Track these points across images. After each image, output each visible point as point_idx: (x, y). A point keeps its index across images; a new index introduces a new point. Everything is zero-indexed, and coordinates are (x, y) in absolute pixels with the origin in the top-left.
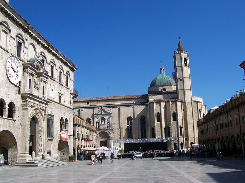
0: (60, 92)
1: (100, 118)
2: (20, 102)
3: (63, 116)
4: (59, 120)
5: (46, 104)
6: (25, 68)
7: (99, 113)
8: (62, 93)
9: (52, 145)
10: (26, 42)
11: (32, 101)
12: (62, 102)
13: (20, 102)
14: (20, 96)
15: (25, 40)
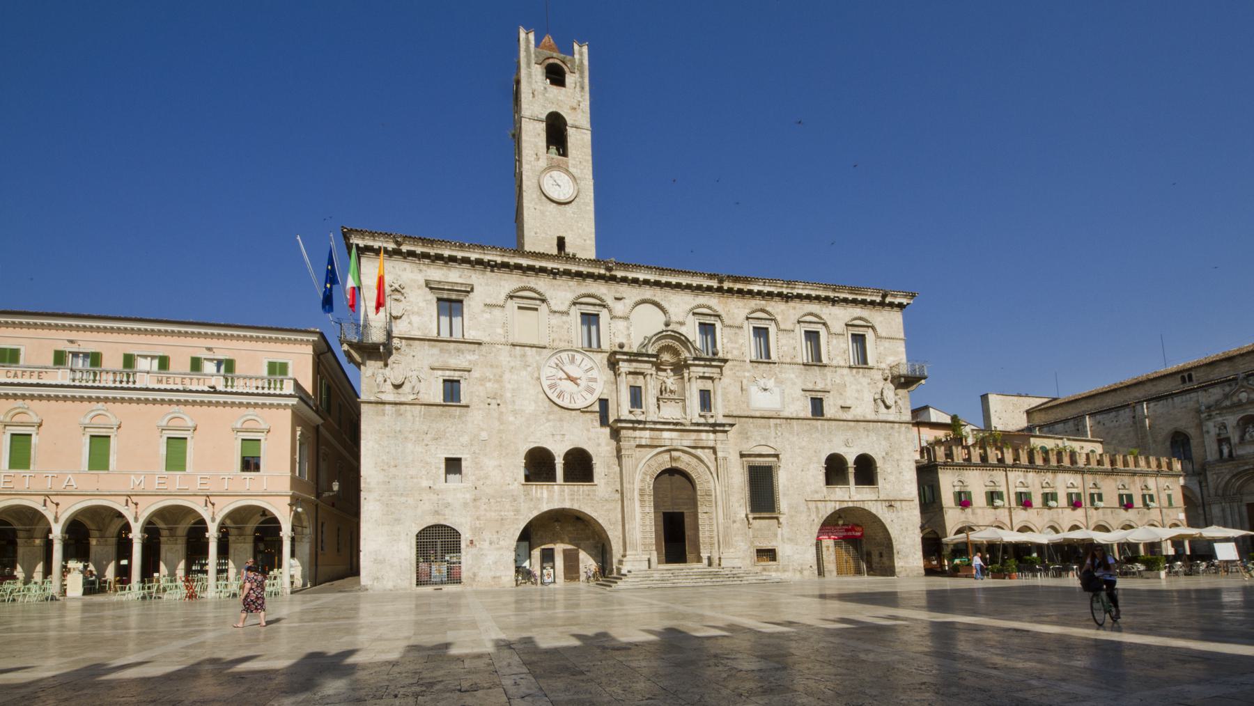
0: (810, 386)
1: (1231, 420)
2: (608, 445)
3: (841, 450)
4: (819, 462)
5: (715, 432)
6: (613, 364)
7: (1228, 403)
8: (828, 388)
9: (784, 531)
10: (619, 308)
11: (647, 434)
12: (830, 409)
13: (608, 445)
14: (608, 430)
15: (610, 301)
